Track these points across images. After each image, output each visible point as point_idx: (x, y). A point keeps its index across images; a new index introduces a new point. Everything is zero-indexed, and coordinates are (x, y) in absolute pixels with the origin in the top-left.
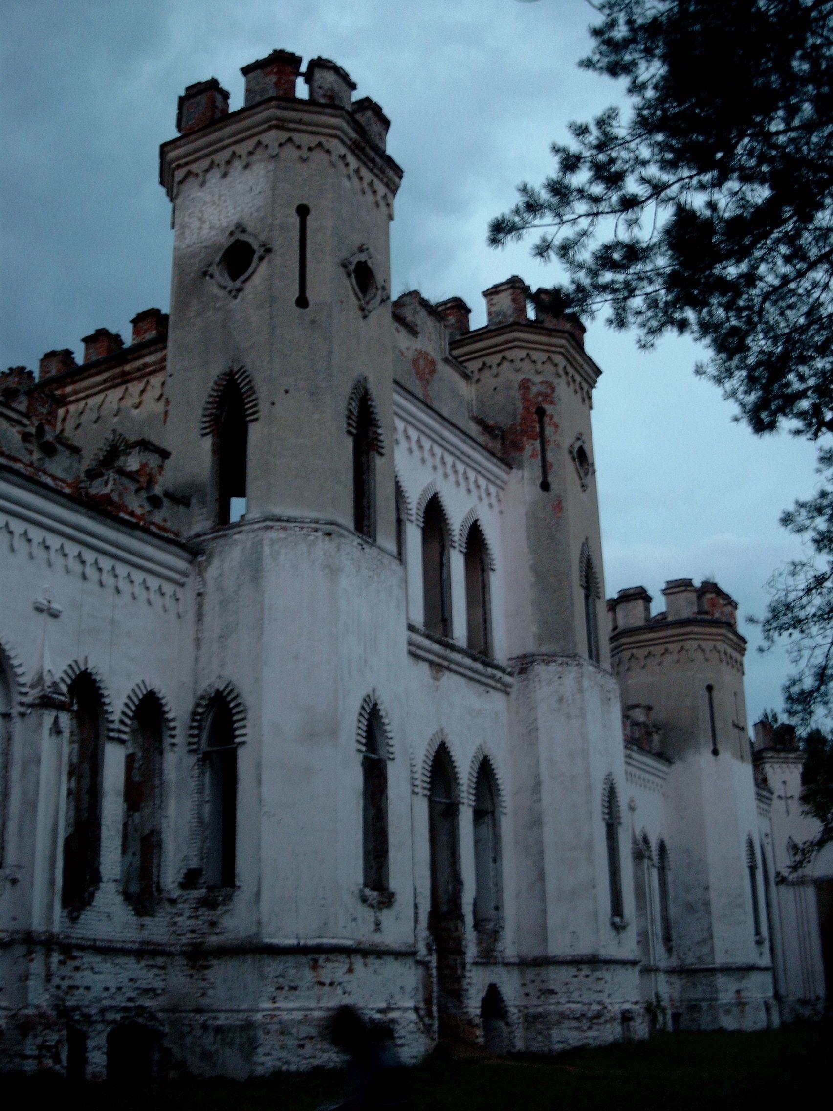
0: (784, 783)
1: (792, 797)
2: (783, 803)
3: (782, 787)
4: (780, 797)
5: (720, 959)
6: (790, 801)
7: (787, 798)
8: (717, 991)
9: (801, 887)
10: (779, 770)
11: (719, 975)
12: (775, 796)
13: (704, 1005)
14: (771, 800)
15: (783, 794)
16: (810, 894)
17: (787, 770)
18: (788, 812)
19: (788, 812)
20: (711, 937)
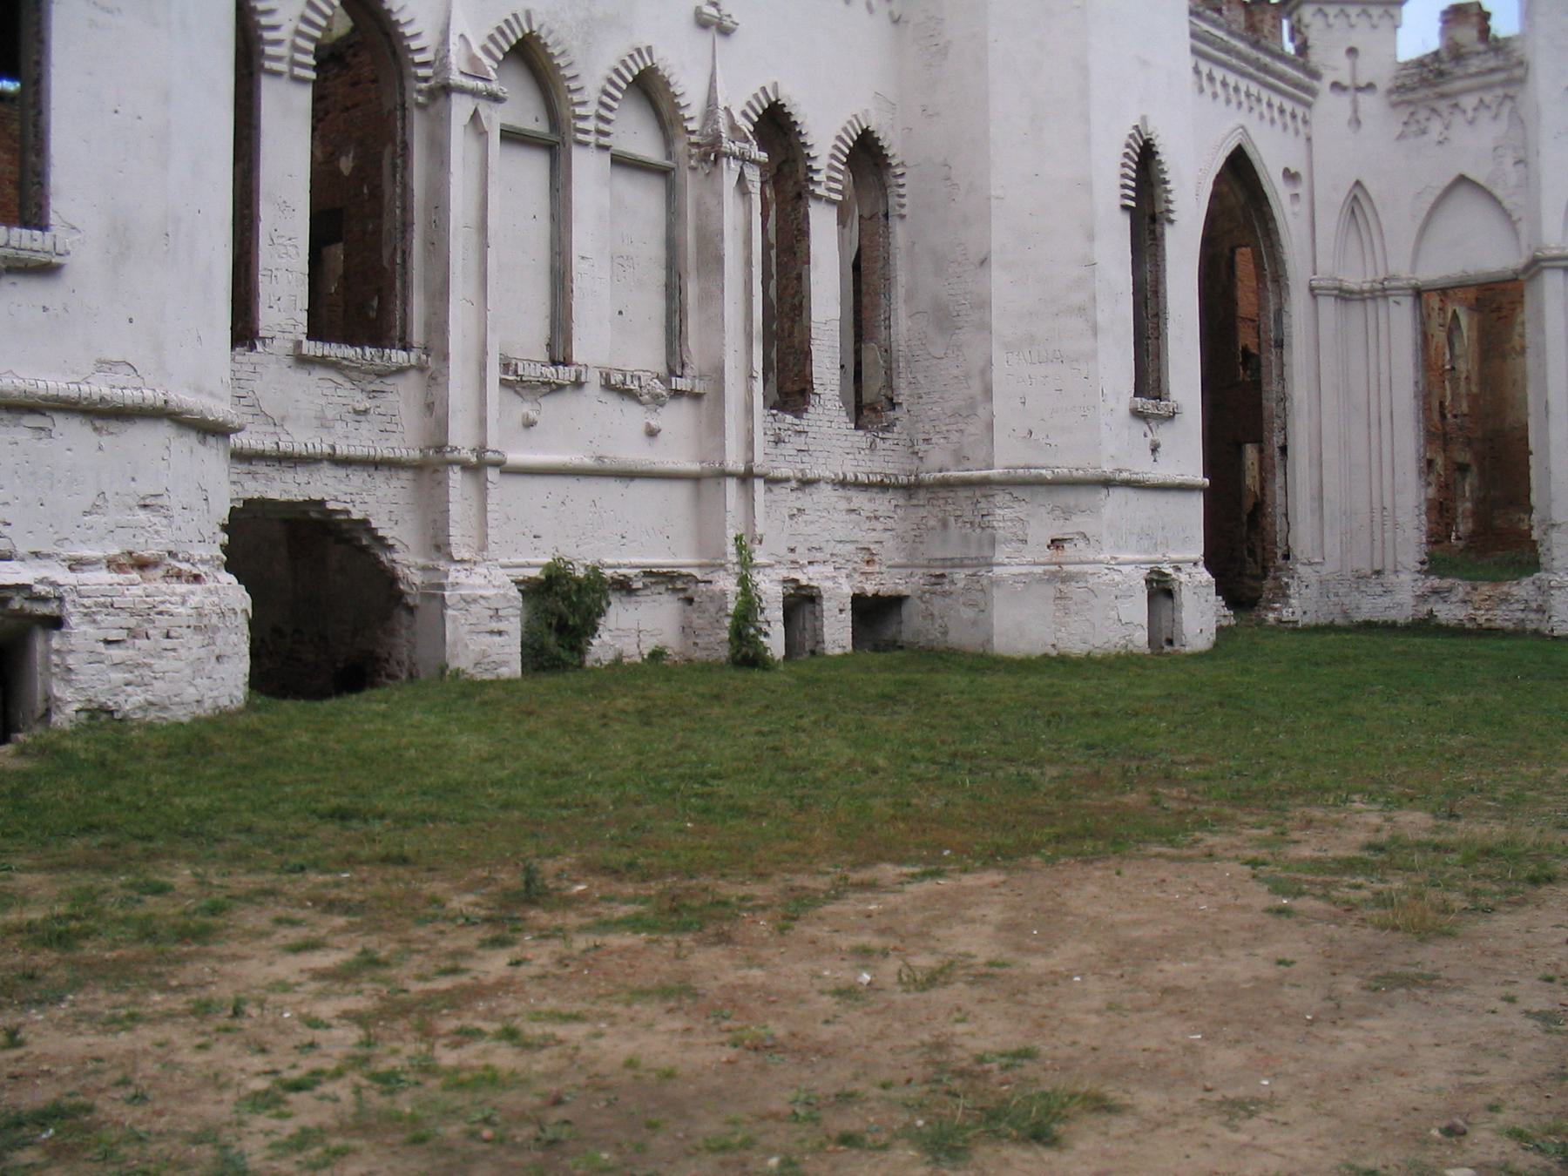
0: (1352, 51)
1: (1370, 86)
2: (1344, 101)
3: (1343, 62)
4: (1336, 86)
5: (1007, 457)
6: (1364, 98)
7: (1359, 89)
8: (993, 542)
9: (1380, 302)
10: (1339, 23)
11: (1001, 498)
12: (1323, 86)
13: (960, 575)
14: (1313, 92)
15: (1346, 81)
16: (1401, 319)
17: (1362, 23)
18: (1356, 122)
19: (1356, 122)
20: (988, 393)
